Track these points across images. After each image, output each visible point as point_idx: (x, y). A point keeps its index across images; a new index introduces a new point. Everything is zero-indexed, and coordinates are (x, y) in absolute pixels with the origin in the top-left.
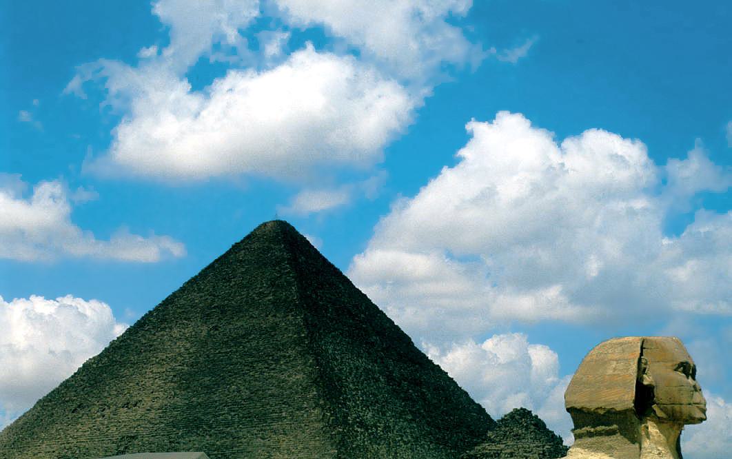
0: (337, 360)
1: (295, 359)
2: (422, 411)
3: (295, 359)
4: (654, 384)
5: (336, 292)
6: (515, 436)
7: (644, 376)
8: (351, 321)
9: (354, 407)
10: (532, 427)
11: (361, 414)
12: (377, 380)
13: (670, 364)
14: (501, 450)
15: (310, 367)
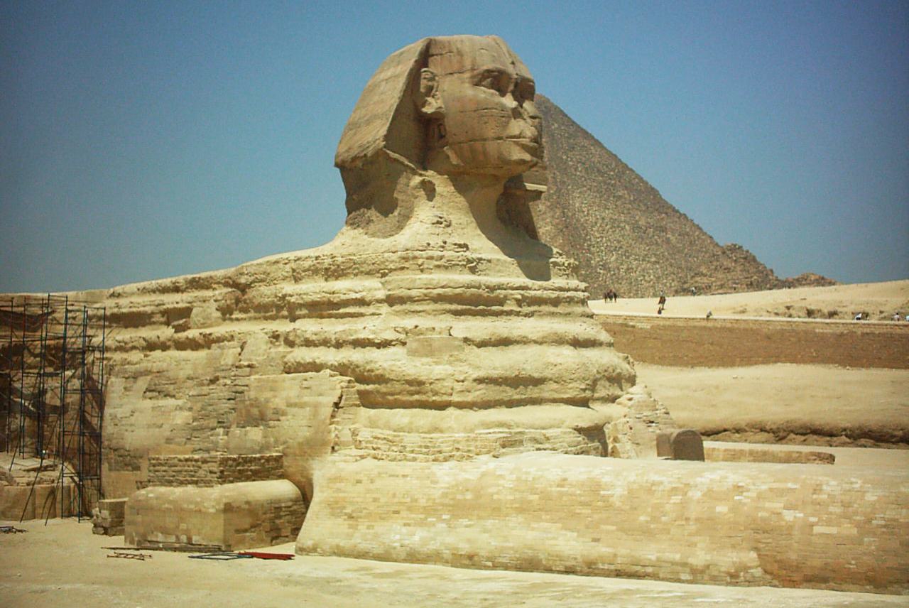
0: (583, 212)
1: (545, 213)
2: (666, 254)
3: (545, 213)
4: (441, 110)
5: (587, 154)
6: (725, 269)
7: (430, 99)
8: (601, 178)
9: (598, 252)
10: (742, 260)
11: (604, 258)
12: (623, 229)
13: (467, 75)
14: (712, 283)
15: (557, 219)
